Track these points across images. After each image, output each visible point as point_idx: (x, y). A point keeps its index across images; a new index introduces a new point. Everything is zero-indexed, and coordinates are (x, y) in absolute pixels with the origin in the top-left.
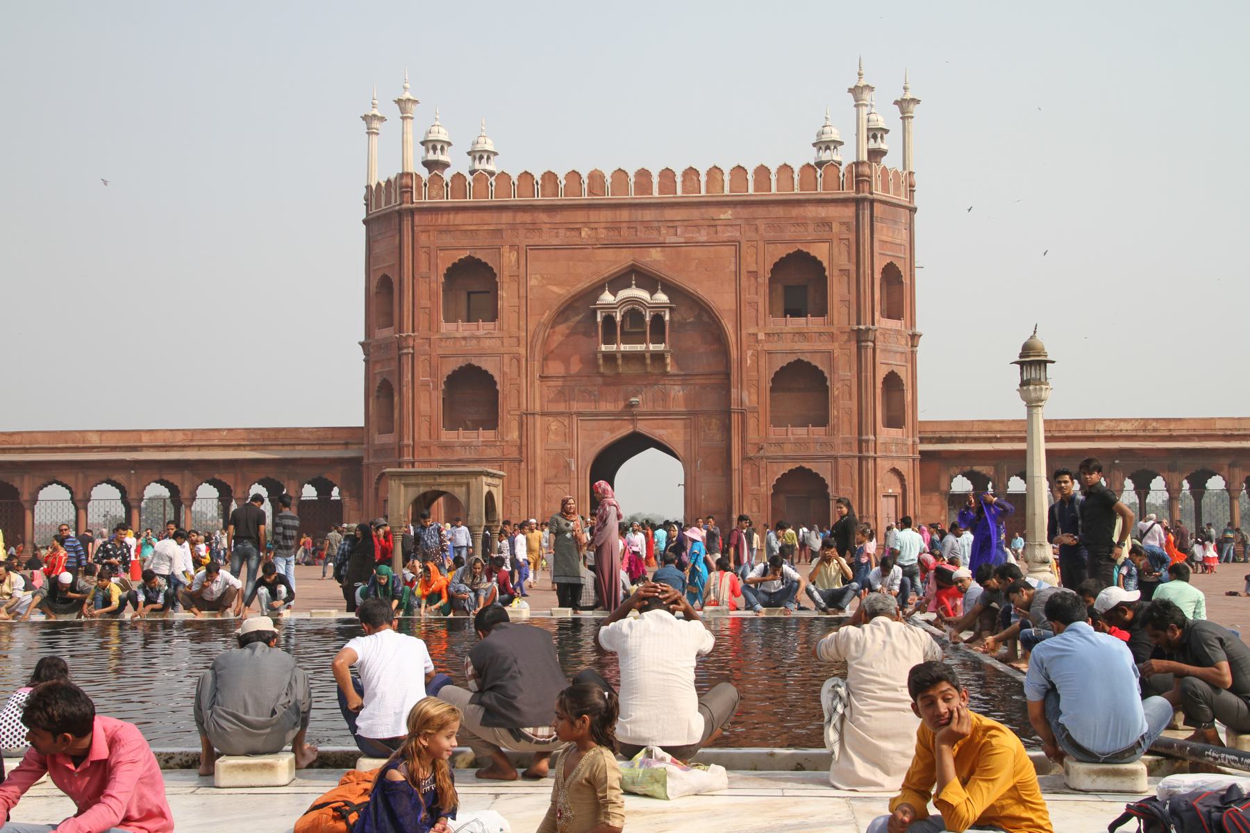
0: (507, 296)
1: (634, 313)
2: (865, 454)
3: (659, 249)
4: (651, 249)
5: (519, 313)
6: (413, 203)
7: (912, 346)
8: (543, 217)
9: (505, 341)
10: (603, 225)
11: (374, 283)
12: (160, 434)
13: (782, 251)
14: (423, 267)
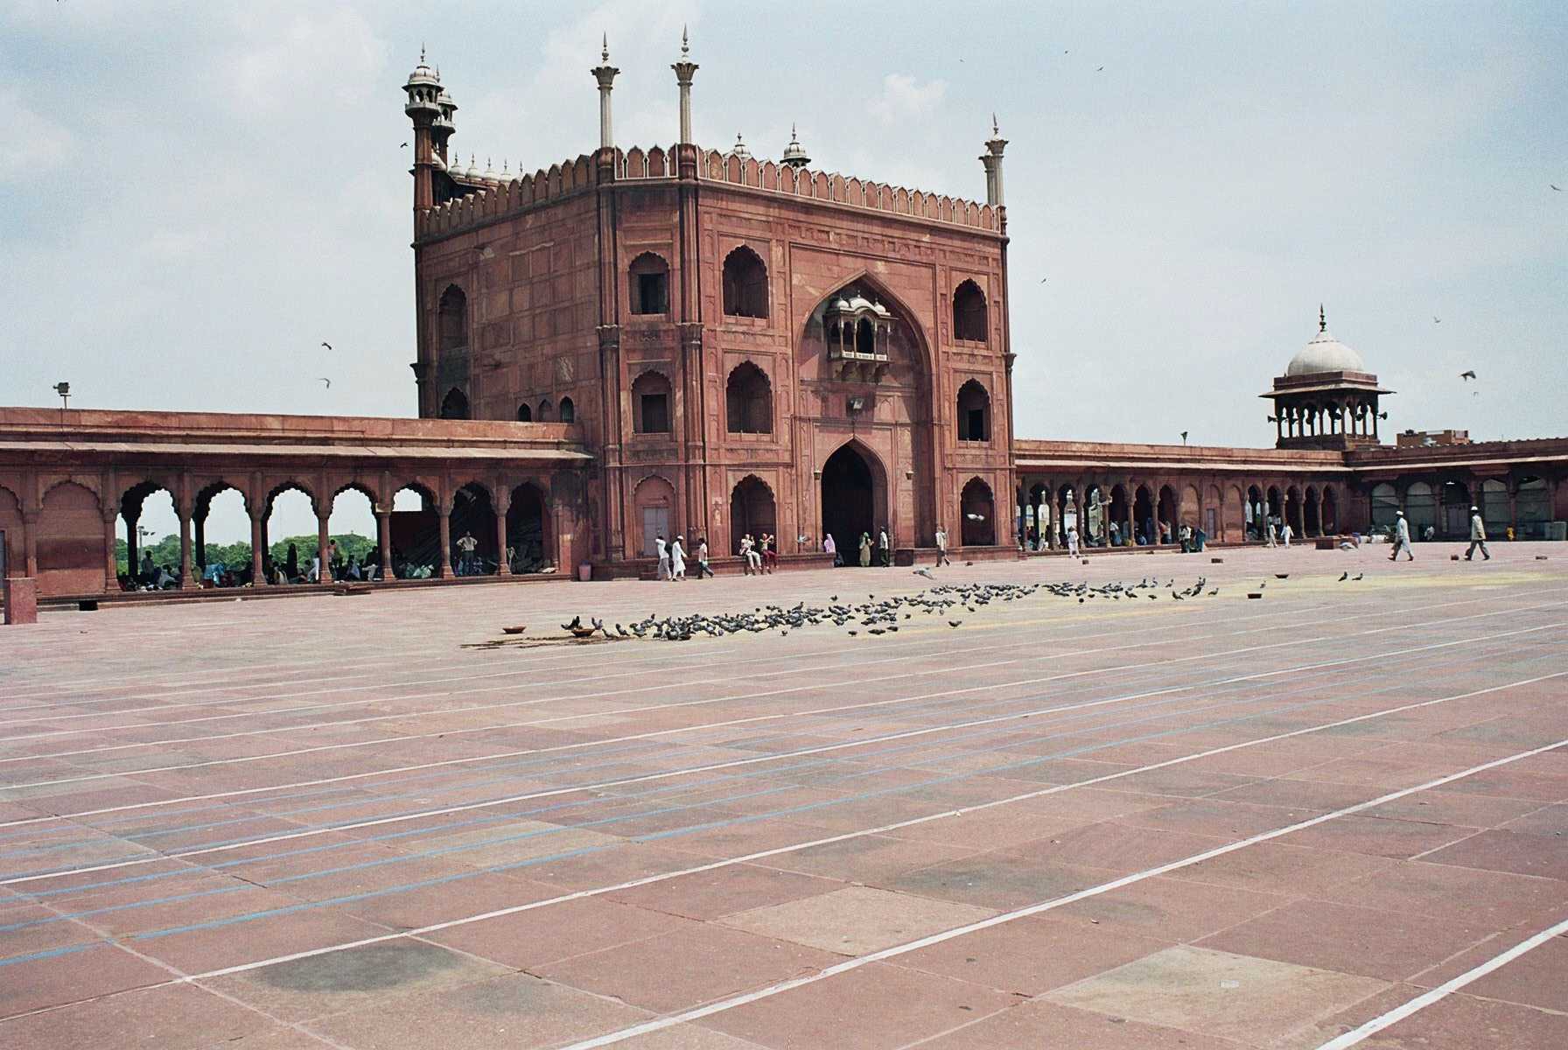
0: (776, 295)
6: (696, 179)
9: (777, 339)
13: (959, 279)
14: (706, 253)
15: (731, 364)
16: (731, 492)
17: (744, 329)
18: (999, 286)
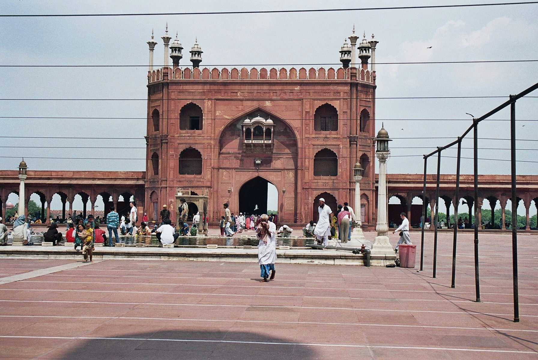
1: (258, 128)
3: (269, 102)
4: (266, 102)
5: (211, 127)
6: (168, 80)
7: (373, 143)
8: (222, 87)
10: (247, 91)
11: (151, 113)
12: (60, 172)
15: (182, 148)
17: (189, 134)
18: (347, 105)
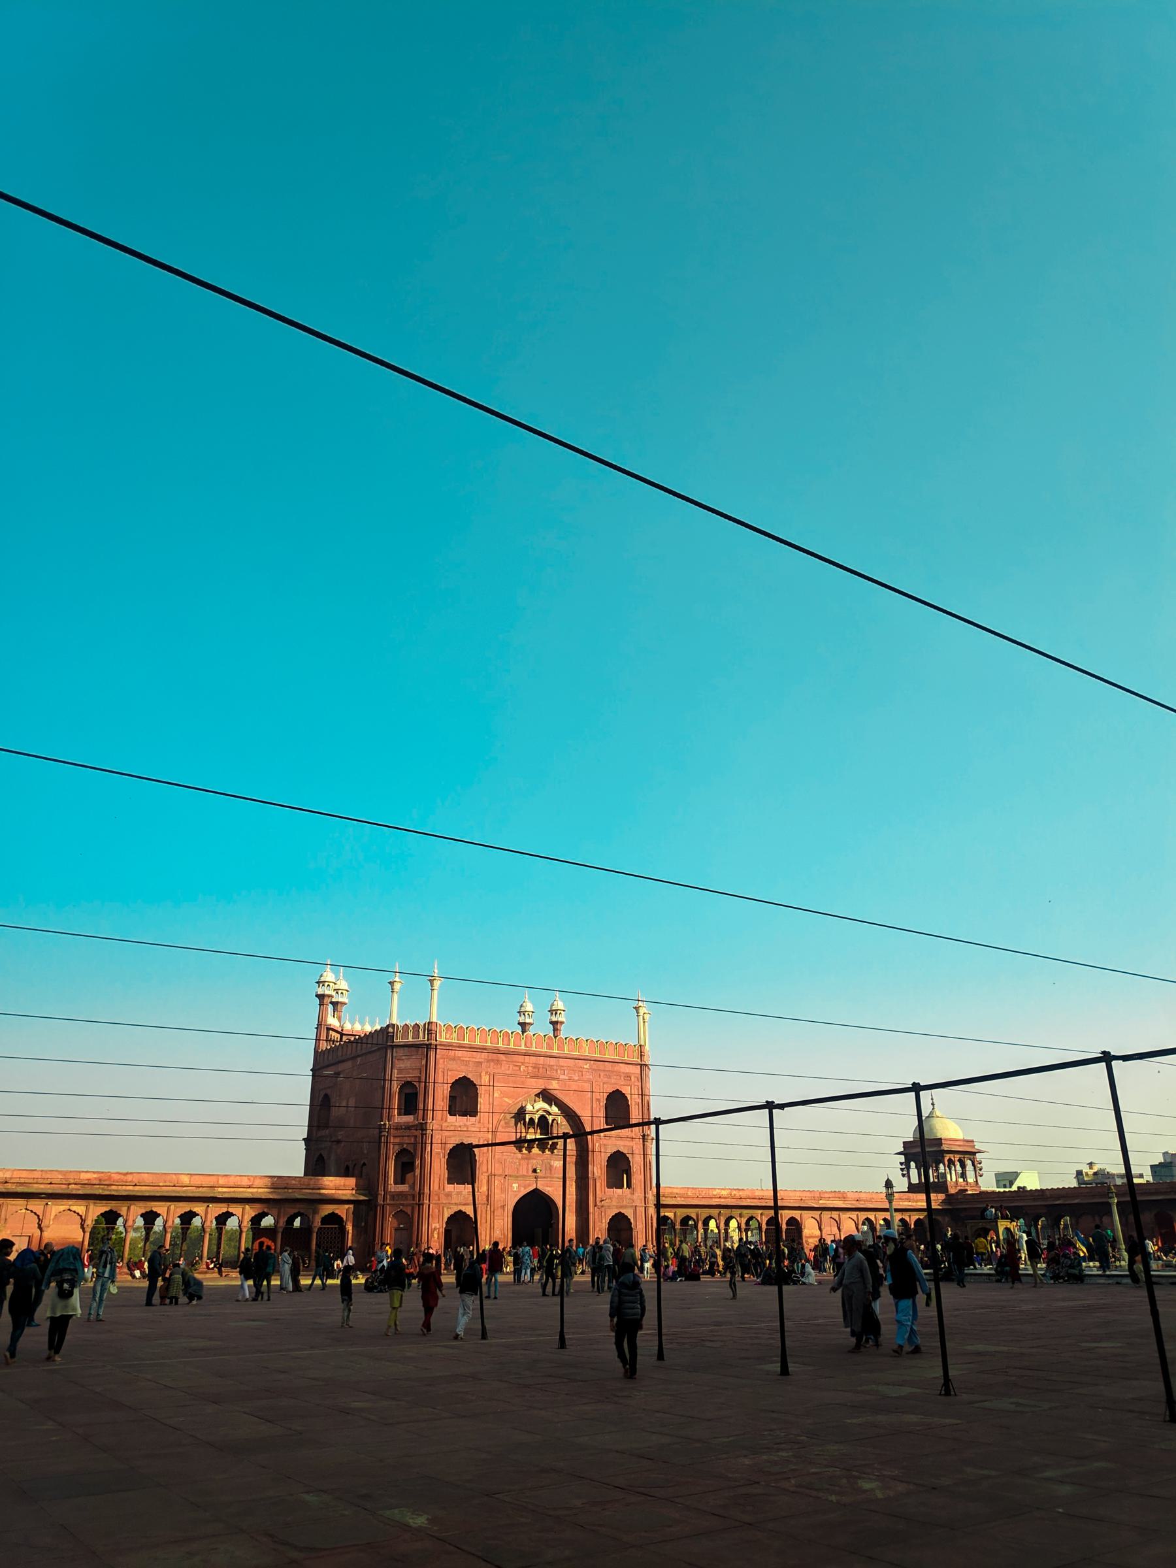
2: (647, 1205)
6: (436, 1041)
8: (502, 1057)
10: (531, 1065)
16: (445, 1220)
